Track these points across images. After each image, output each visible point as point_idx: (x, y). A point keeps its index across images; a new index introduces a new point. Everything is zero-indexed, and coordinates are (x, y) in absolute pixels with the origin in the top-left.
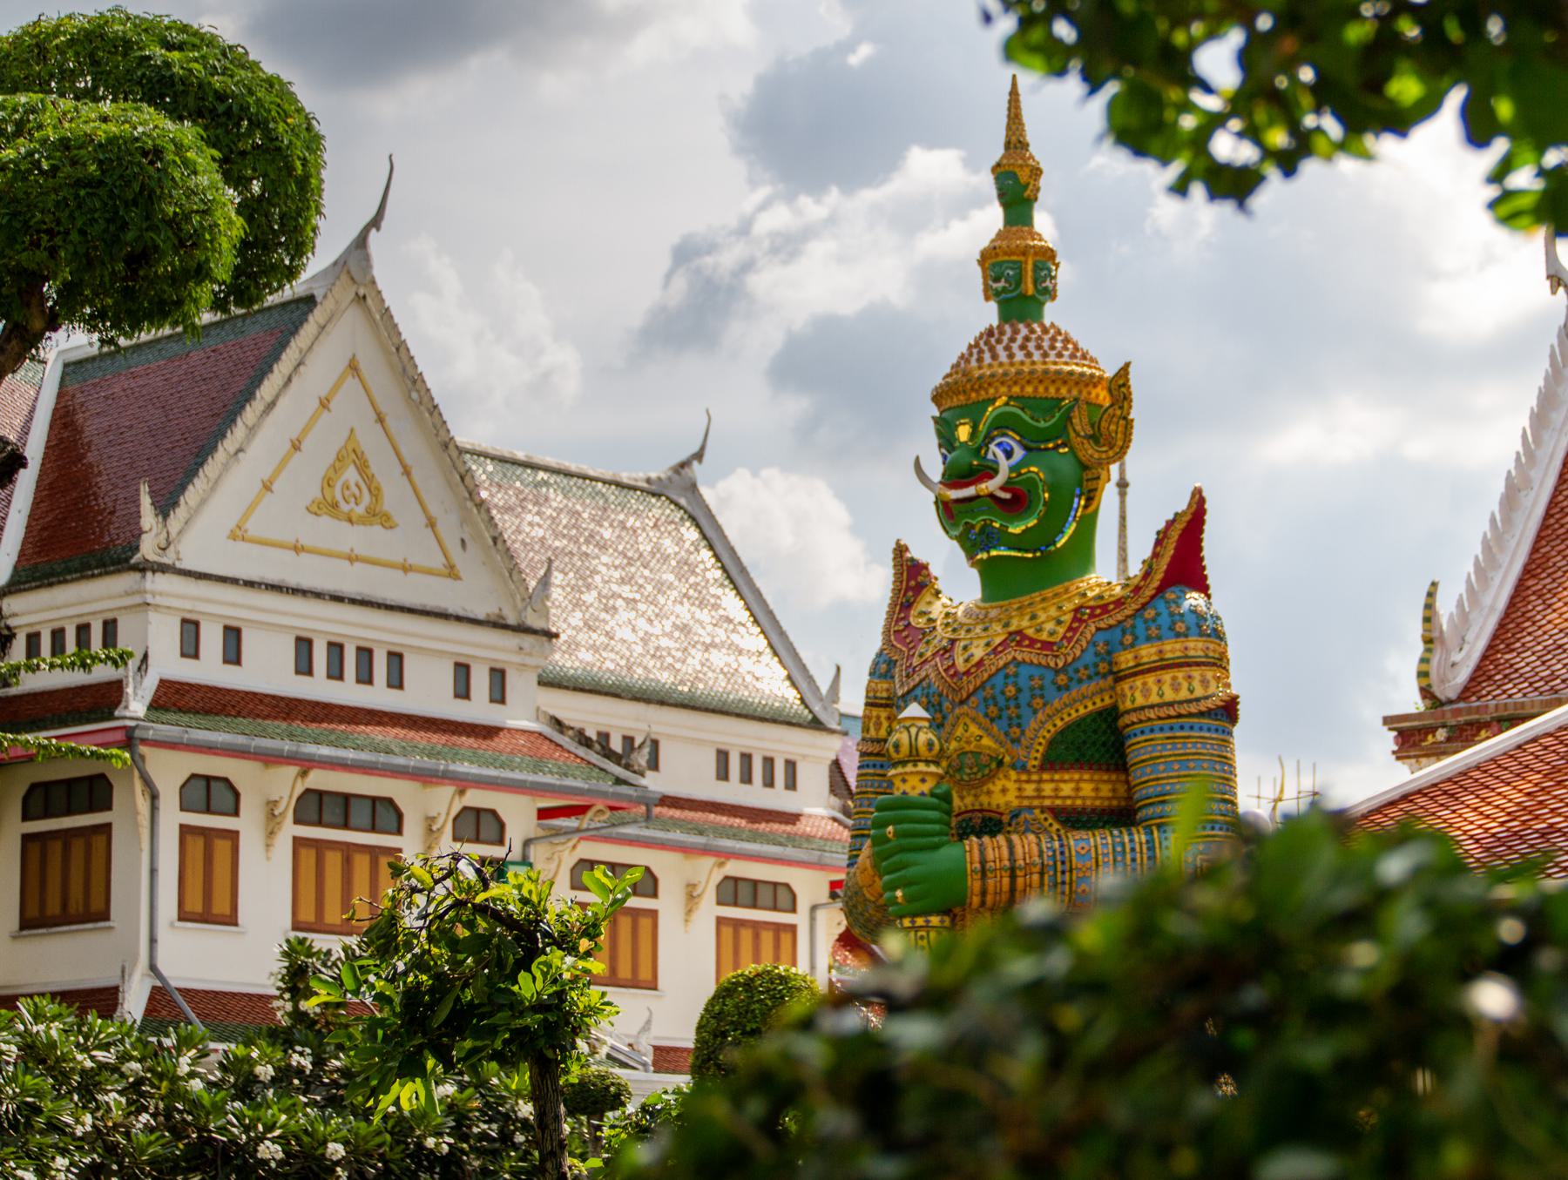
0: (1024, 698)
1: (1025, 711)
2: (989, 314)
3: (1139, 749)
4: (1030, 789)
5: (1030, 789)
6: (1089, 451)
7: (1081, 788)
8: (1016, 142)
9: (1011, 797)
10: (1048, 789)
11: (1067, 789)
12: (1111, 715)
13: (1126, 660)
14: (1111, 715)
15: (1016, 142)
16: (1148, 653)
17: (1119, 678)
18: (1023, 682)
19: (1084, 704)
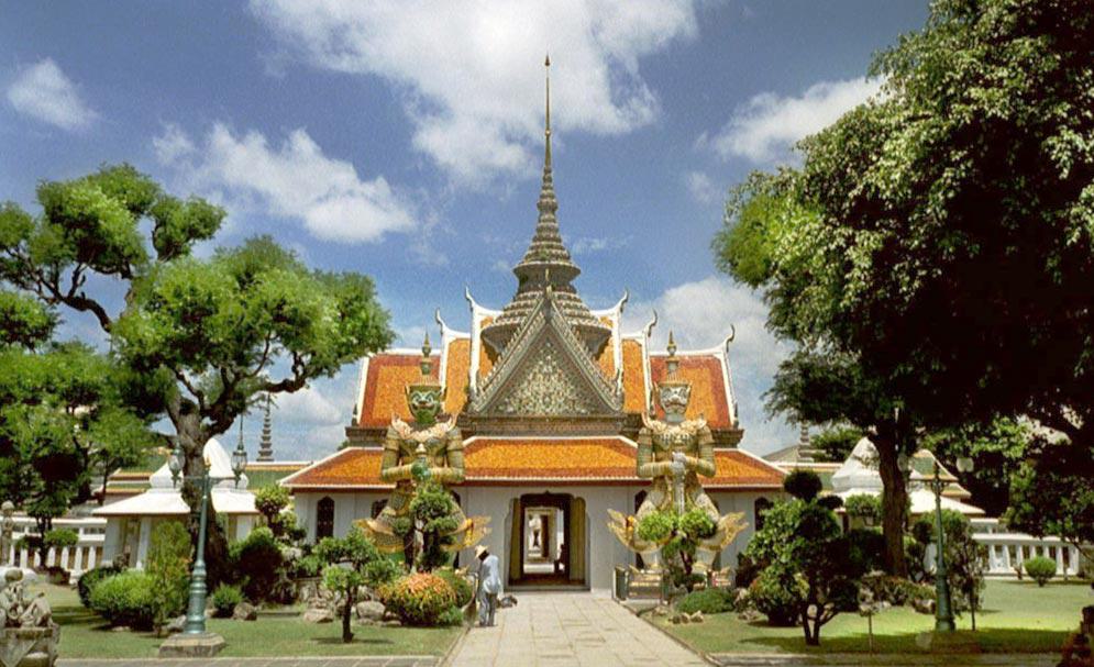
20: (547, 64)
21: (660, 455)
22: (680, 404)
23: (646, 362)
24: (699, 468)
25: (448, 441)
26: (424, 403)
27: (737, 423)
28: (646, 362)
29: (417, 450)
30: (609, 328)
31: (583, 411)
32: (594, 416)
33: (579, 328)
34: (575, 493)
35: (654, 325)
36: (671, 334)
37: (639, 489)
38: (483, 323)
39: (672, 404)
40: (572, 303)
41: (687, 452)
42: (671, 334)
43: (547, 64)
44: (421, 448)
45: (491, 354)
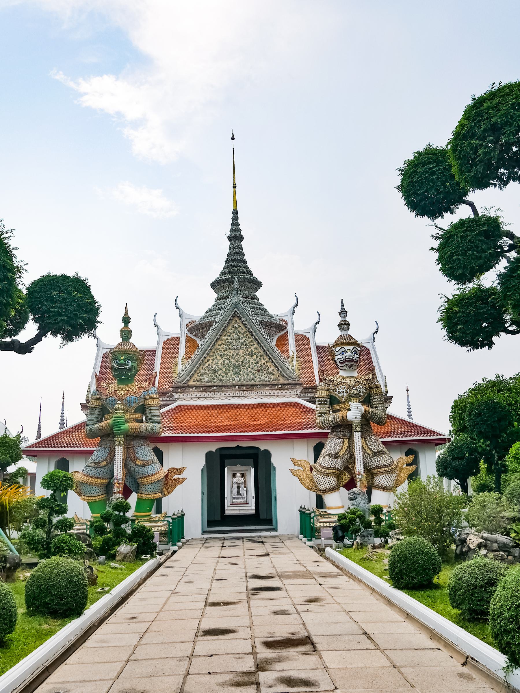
0: (132, 401)
1: (132, 403)
2: (121, 340)
3: (149, 411)
4: (131, 416)
5: (131, 416)
6: (139, 363)
7: (138, 416)
8: (126, 313)
9: (128, 417)
10: (134, 416)
11: (137, 416)
12: (144, 405)
13: (148, 397)
14: (144, 405)
15: (126, 313)
16: (151, 396)
17: (146, 399)
18: (133, 399)
19: (141, 402)
20: (233, 139)
21: (336, 407)
22: (353, 360)
23: (313, 350)
24: (373, 414)
25: (146, 399)
26: (121, 365)
27: (387, 392)
28: (313, 350)
29: (117, 406)
30: (284, 324)
31: (267, 379)
32: (275, 382)
33: (261, 322)
34: (263, 446)
35: (318, 323)
36: (342, 300)
37: (315, 442)
38: (187, 325)
39: (346, 361)
40: (255, 306)
41: (363, 402)
42: (342, 300)
43: (233, 139)
44: (119, 405)
45: (192, 345)
